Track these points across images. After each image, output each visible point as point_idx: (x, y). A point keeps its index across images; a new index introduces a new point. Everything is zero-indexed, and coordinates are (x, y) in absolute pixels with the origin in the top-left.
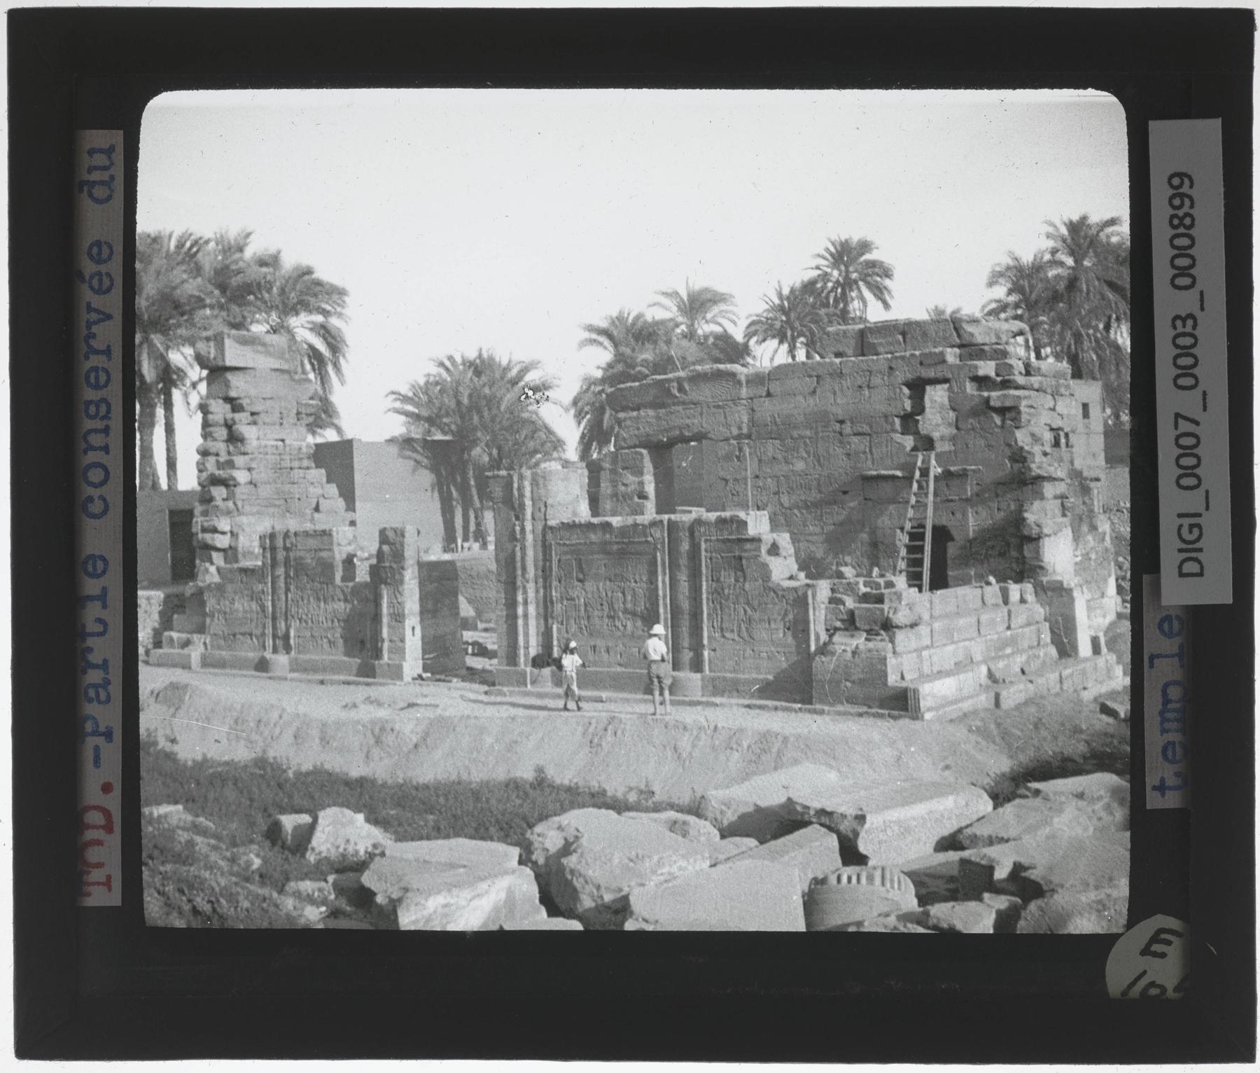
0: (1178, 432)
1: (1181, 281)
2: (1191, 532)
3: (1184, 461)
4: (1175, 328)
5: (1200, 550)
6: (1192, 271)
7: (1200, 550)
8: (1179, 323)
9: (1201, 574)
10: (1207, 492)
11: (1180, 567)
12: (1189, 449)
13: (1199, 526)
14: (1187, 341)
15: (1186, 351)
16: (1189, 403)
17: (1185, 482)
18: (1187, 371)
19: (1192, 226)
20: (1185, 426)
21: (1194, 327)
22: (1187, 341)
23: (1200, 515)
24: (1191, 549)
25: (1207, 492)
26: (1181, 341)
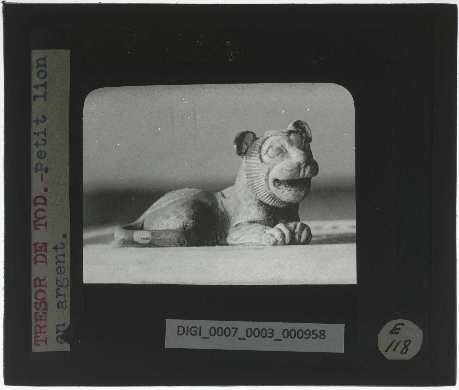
0: (231, 328)
1: (286, 333)
2: (194, 331)
3: (220, 330)
4: (269, 329)
5: (187, 334)
6: (289, 337)
7: (187, 334)
8: (271, 331)
9: (179, 334)
10: (208, 338)
11: (181, 327)
12: (224, 332)
13: (196, 334)
14: (264, 335)
15: (260, 333)
16: (241, 333)
17: (213, 330)
18: (253, 333)
19: (321, 338)
20: (233, 331)
21: (268, 337)
22: (264, 335)
23: (200, 335)
24: (188, 331)
25: (208, 338)
26: (264, 332)
